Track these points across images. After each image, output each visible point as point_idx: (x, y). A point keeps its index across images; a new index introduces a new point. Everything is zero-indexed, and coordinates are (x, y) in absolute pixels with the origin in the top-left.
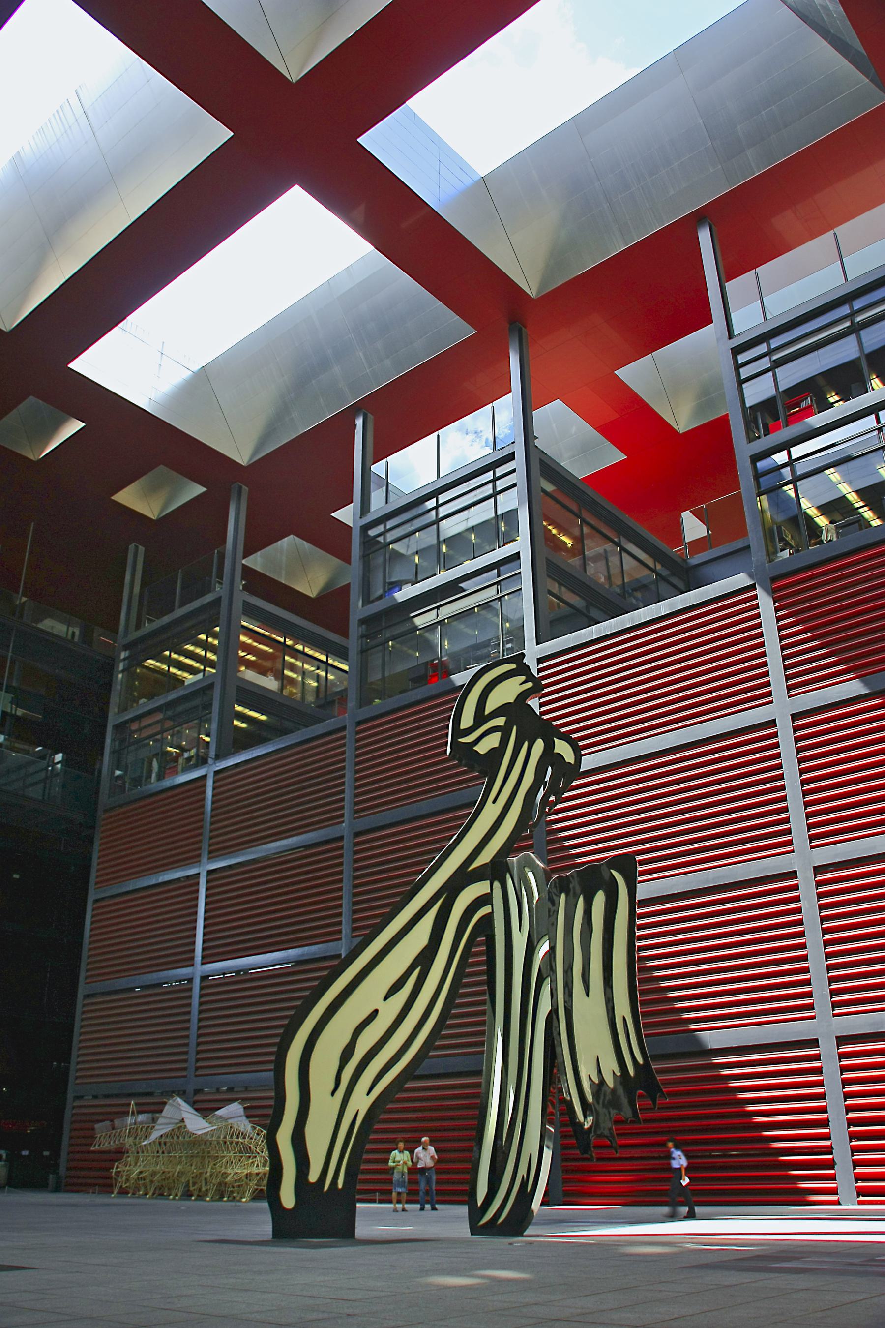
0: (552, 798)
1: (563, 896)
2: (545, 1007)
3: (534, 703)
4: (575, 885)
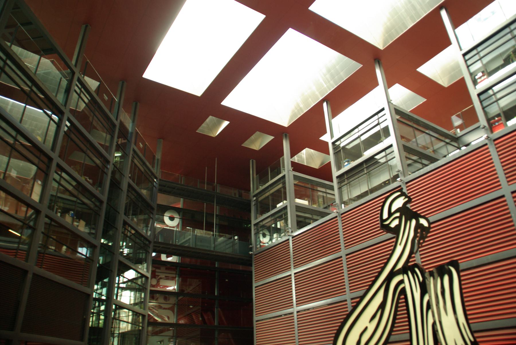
0: (421, 241)
1: (432, 279)
2: (431, 321)
3: (408, 206)
4: (436, 275)
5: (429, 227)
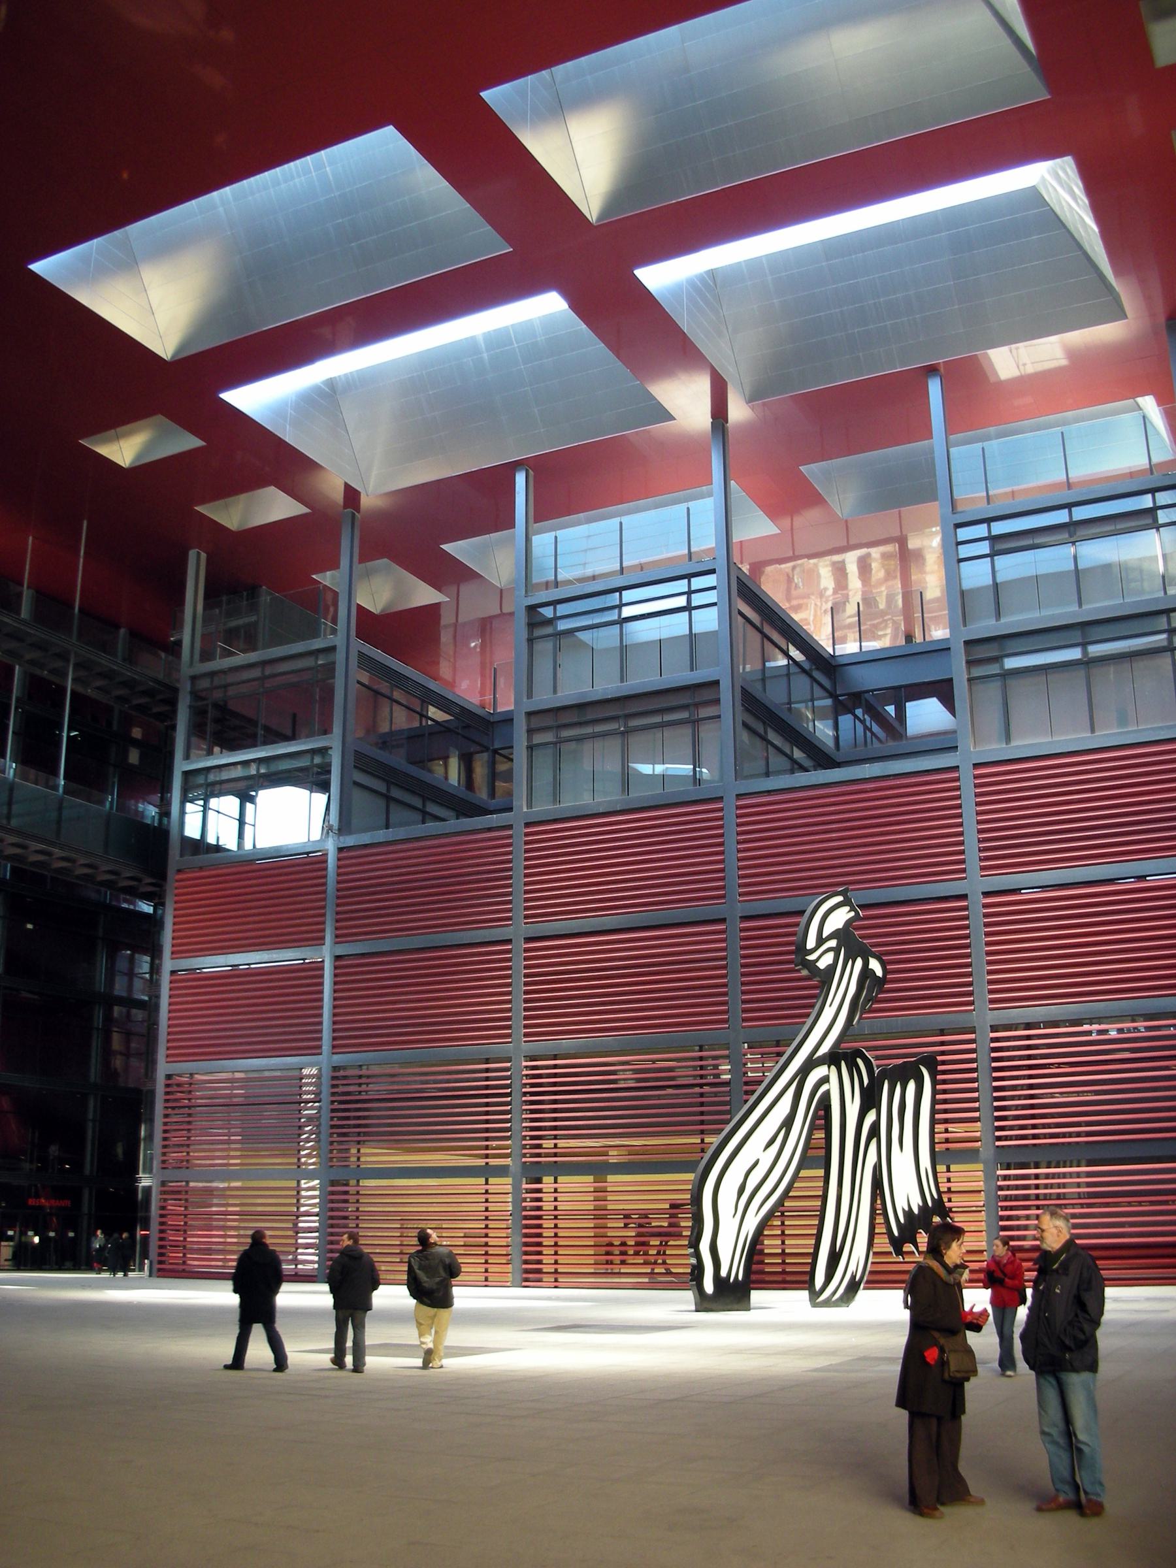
5: (883, 980)
